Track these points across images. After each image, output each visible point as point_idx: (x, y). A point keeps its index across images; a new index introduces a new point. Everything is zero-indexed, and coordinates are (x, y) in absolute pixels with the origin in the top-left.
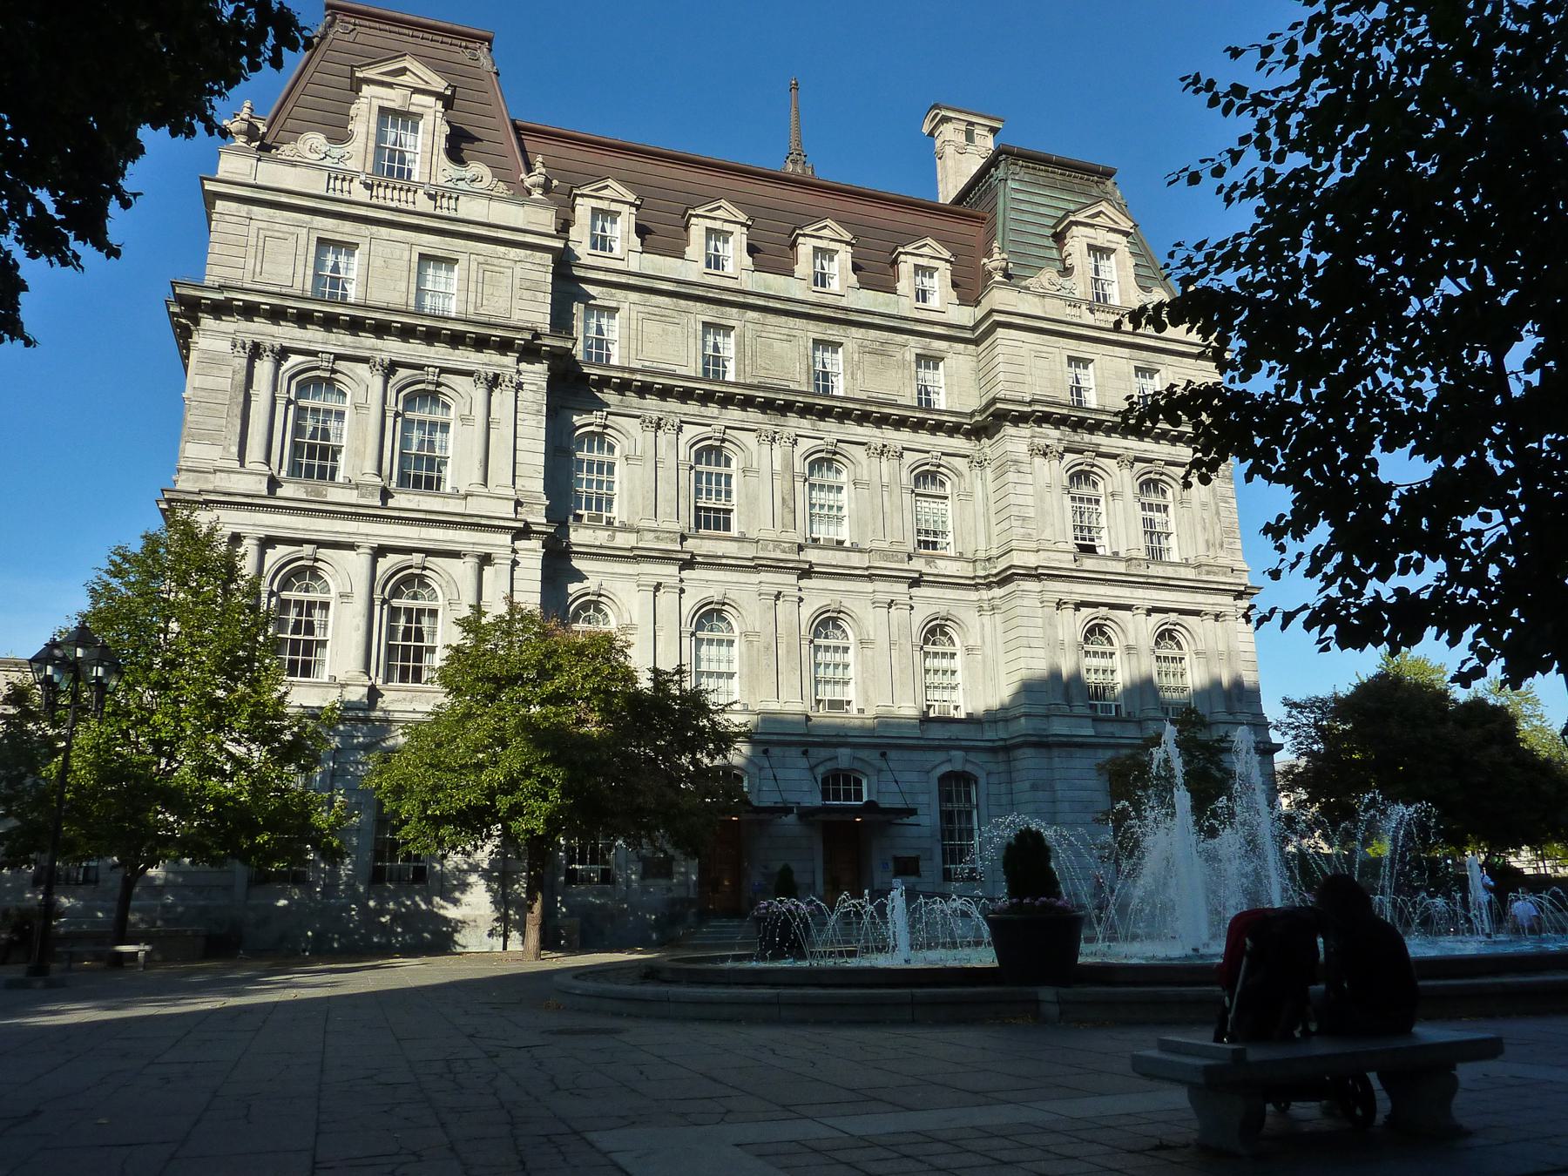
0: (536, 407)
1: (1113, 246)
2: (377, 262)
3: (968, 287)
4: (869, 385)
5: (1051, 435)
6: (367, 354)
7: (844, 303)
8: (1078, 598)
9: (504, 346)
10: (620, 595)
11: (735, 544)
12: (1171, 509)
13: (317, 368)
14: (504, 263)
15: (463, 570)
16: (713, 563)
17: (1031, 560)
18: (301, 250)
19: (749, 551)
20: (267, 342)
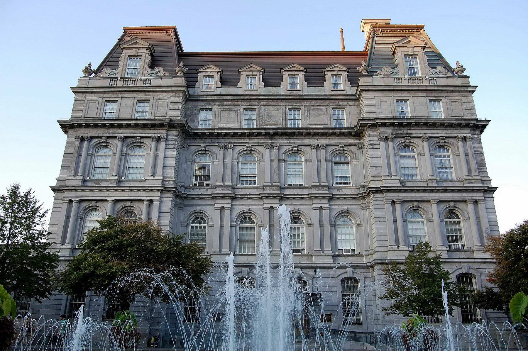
0: (173, 146)
1: (417, 53)
2: (123, 105)
3: (353, 81)
4: (312, 123)
5: (388, 132)
6: (116, 135)
7: (301, 93)
8: (402, 199)
9: (162, 126)
10: (208, 212)
11: (255, 190)
12: (451, 156)
13: (102, 142)
14: (165, 98)
15: (144, 206)
16: (244, 197)
17: (378, 184)
18: (100, 105)
19: (259, 191)
20: (85, 136)
